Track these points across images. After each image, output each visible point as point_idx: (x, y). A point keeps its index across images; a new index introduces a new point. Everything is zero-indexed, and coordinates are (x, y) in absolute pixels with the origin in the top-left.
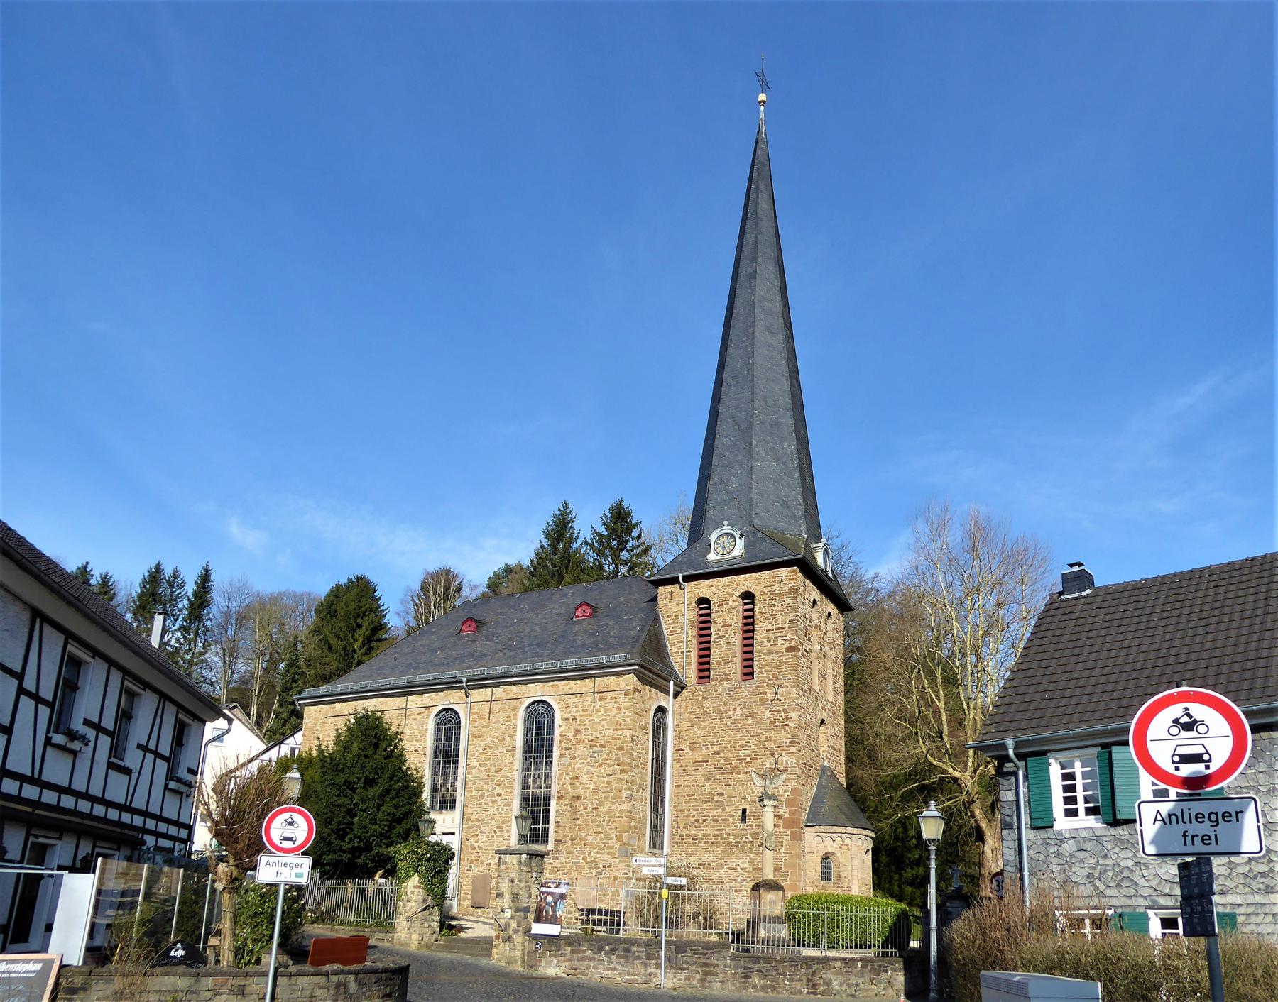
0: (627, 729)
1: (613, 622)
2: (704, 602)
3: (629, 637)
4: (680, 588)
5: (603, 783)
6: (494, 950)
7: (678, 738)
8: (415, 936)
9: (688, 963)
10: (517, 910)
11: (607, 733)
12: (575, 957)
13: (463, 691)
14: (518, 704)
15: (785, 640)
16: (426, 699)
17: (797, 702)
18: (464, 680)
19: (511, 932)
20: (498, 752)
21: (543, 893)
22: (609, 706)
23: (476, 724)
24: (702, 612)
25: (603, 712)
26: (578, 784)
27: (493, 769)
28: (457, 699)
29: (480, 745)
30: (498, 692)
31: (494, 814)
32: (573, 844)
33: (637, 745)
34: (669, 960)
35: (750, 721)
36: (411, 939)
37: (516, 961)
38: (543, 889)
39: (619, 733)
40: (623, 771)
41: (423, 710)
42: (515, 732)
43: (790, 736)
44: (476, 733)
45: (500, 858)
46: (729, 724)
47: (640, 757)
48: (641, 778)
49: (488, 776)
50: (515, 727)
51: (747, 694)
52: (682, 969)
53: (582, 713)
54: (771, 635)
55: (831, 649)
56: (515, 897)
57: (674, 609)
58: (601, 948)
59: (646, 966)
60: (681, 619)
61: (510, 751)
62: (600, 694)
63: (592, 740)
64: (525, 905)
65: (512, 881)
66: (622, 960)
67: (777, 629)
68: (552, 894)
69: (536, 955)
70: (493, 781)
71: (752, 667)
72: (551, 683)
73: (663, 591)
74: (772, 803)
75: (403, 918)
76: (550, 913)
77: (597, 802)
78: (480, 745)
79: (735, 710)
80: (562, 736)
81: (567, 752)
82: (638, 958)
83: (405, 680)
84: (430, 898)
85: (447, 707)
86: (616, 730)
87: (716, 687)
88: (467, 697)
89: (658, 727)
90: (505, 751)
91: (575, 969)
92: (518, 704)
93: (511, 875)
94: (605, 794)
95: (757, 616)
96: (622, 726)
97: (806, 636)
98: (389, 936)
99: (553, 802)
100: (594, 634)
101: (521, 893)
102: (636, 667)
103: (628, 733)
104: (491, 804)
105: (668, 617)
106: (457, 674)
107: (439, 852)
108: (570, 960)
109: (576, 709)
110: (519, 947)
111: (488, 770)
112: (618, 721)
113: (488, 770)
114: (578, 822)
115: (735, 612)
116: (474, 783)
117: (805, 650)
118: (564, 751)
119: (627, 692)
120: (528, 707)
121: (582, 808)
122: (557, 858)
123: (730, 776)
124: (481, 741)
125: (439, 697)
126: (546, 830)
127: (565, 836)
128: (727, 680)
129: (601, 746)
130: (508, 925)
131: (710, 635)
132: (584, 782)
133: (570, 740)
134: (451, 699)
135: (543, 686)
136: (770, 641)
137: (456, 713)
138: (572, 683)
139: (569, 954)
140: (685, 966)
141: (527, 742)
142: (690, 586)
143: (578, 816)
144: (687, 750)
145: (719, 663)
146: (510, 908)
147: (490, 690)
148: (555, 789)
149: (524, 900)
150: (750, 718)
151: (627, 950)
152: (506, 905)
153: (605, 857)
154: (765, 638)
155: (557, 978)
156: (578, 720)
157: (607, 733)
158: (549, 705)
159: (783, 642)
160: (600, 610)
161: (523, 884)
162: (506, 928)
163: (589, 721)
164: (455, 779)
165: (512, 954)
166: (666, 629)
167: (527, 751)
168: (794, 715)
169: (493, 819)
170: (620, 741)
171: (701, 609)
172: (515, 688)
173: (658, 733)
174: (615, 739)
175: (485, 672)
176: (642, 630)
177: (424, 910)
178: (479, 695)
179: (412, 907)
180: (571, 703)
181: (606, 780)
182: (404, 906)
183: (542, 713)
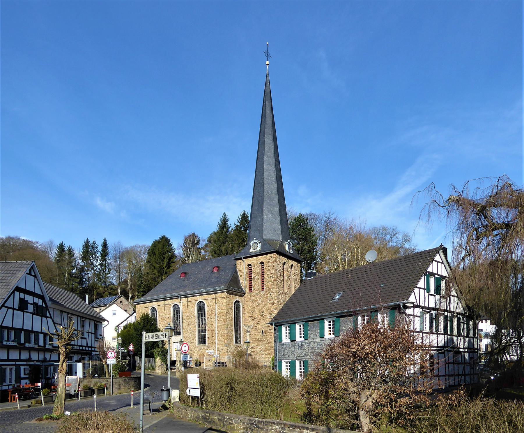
16: (170, 302)
18: (179, 296)
23: (184, 309)
27: (190, 322)
35: (264, 304)
39: (223, 310)
40: (224, 322)
48: (230, 323)
55: (294, 276)
57: (241, 268)
62: (217, 299)
74: (249, 333)
75: (157, 367)
81: (209, 317)
83: (163, 296)
86: (222, 310)
87: (254, 293)
95: (265, 270)
99: (207, 332)
106: (177, 294)
111: (188, 323)
113: (188, 323)
114: (214, 337)
115: (258, 269)
116: (185, 327)
119: (224, 298)
120: (198, 303)
126: (205, 340)
127: (210, 342)
128: (257, 291)
130: (179, 368)
131: (252, 276)
134: (176, 302)
141: (199, 314)
142: (245, 260)
144: (247, 313)
145: (254, 285)
147: (187, 298)
148: (207, 328)
152: (178, 363)
153: (221, 347)
160: (221, 269)
164: (180, 326)
168: (276, 301)
175: (185, 293)
176: (231, 276)
178: (185, 300)
180: (209, 302)
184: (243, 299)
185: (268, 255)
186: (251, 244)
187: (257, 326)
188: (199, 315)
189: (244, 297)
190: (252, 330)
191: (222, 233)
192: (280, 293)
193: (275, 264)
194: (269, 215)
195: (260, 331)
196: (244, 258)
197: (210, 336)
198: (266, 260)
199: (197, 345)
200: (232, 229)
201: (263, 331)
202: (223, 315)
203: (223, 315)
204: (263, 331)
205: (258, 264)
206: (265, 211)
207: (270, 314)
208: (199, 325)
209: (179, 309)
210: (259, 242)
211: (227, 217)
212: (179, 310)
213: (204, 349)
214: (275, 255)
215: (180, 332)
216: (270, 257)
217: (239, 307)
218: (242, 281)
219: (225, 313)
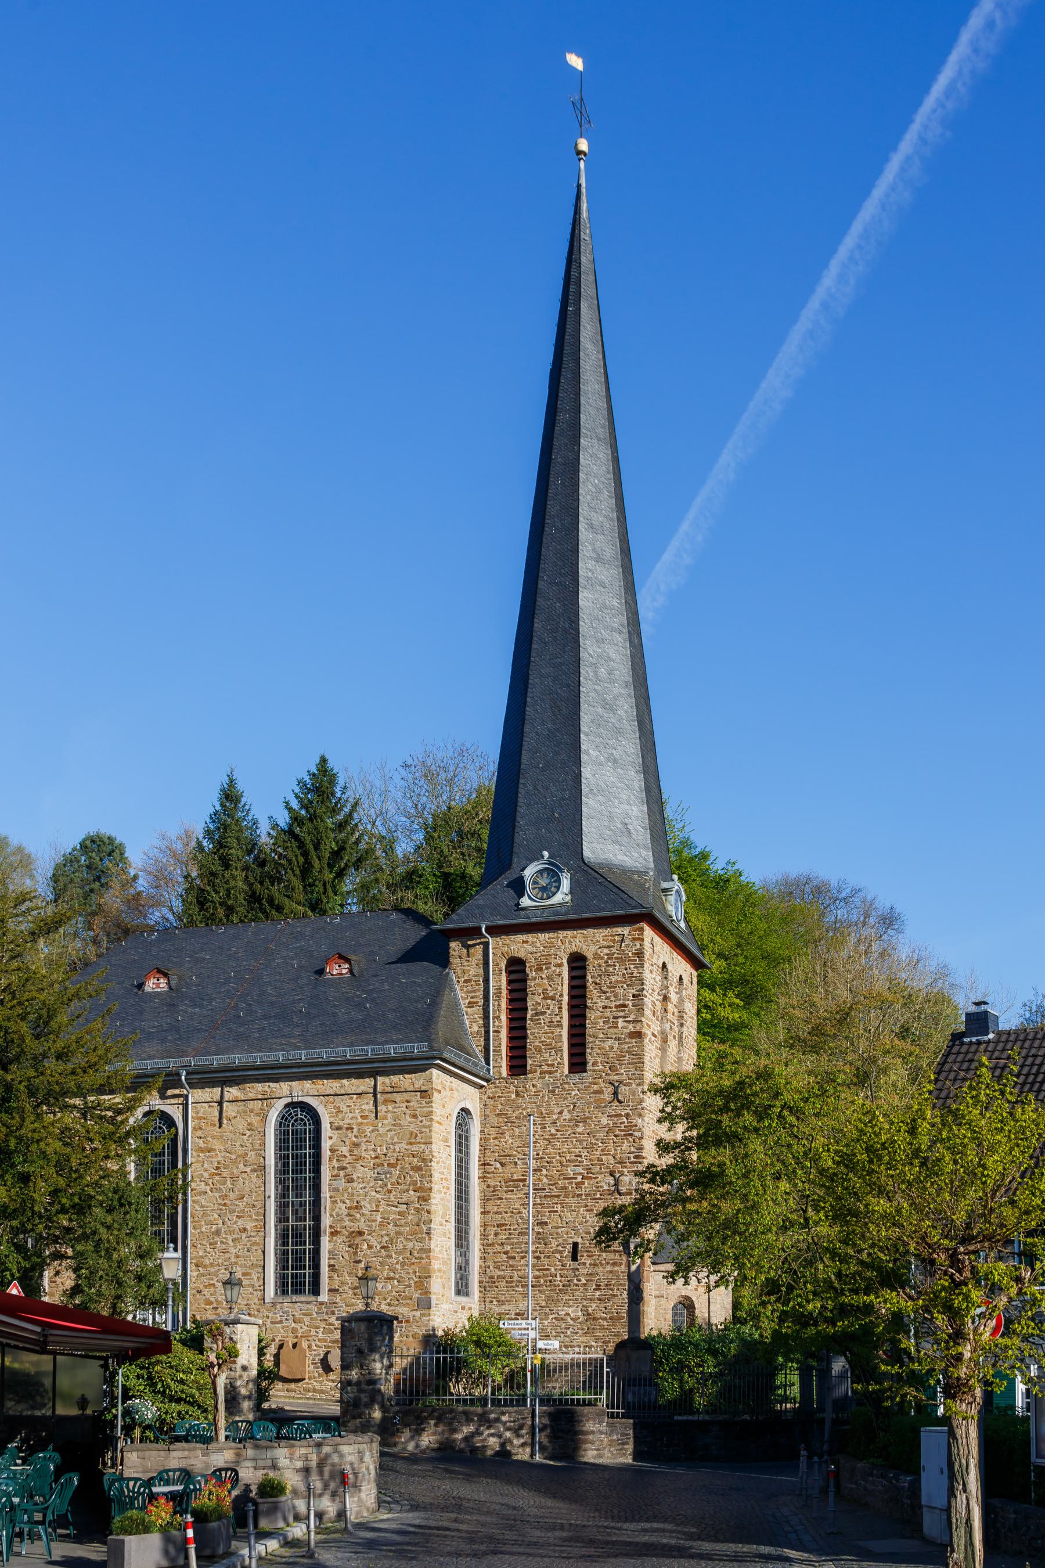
7: (484, 1148)
35: (580, 1129)
39: (415, 1148)
43: (633, 1149)
46: (553, 1131)
47: (442, 1179)
63: (376, 1157)
67: (616, 1007)
70: (232, 1211)
79: (561, 1113)
81: (342, 1173)
86: (411, 1144)
87: (534, 1081)
89: (460, 1136)
90: (248, 1169)
95: (590, 986)
96: (418, 1139)
100: (360, 1005)
104: (231, 1244)
109: (351, 1115)
112: (412, 1133)
117: (654, 1035)
118: (336, 1172)
122: (333, 1313)
123: (555, 1200)
128: (550, 1073)
133: (345, 1156)
141: (282, 1159)
145: (538, 1050)
150: (581, 1125)
156: (355, 1130)
159: (626, 1024)
167: (282, 1172)
172: (259, 1086)
183: (302, 1120)
201: (575, 1245)
204: (575, 1245)
207: (612, 1174)
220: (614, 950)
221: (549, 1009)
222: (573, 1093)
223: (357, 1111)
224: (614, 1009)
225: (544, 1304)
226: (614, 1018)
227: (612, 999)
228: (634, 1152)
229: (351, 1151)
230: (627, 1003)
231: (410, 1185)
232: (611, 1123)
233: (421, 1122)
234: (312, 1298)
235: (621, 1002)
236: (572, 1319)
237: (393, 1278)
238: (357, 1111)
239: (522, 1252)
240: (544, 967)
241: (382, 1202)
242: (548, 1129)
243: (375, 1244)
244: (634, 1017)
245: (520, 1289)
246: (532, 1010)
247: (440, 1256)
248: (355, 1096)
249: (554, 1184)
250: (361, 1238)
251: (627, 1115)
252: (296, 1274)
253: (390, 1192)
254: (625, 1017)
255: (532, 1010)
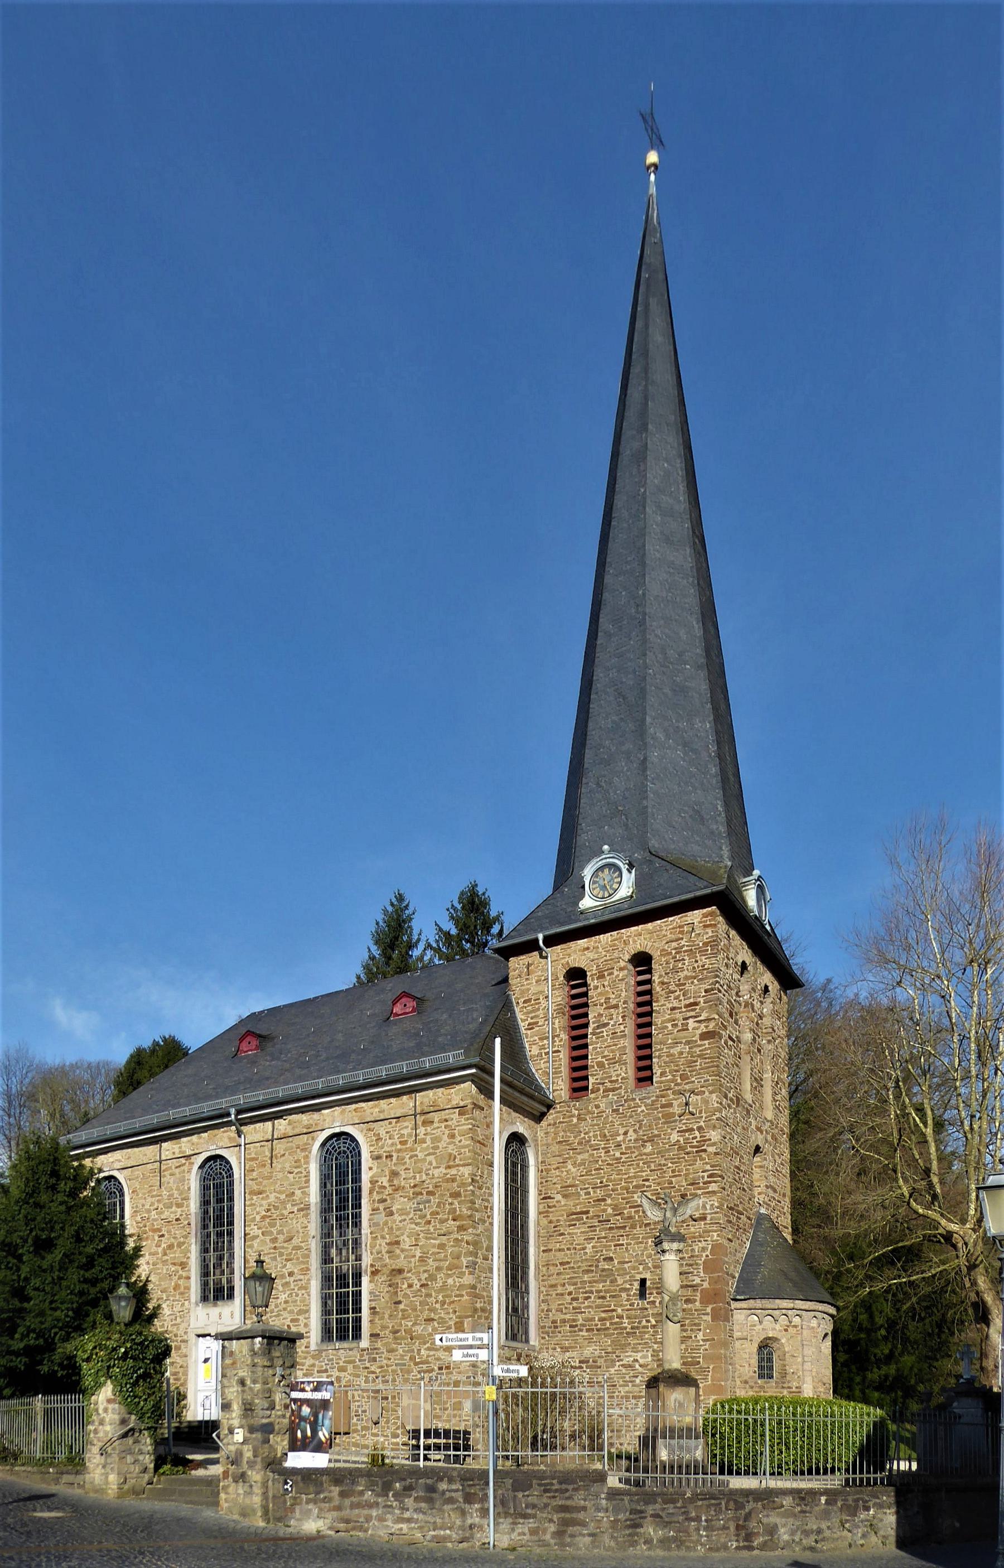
0: (464, 1165)
1: (445, 1016)
2: (576, 975)
3: (466, 1032)
4: (541, 957)
5: (434, 1246)
6: (223, 1496)
8: (112, 1478)
9: (534, 1506)
10: (252, 1430)
11: (436, 1173)
12: (347, 1502)
13: (233, 1128)
14: (310, 1141)
15: (699, 1022)
16: (185, 1144)
17: (718, 1115)
18: (233, 1111)
19: (245, 1466)
20: (286, 1213)
21: (295, 1401)
22: (438, 1132)
23: (255, 1174)
24: (574, 992)
25: (429, 1142)
26: (398, 1251)
27: (281, 1238)
28: (226, 1140)
29: (261, 1205)
30: (282, 1125)
31: (286, 1302)
32: (395, 1338)
33: (480, 1188)
34: (501, 1502)
35: (649, 1148)
36: (107, 1483)
37: (254, 1511)
38: (295, 1395)
39: (454, 1171)
40: (461, 1228)
41: (183, 1160)
42: (308, 1181)
43: (708, 1167)
44: (255, 1187)
45: (223, 1347)
46: (618, 1155)
49: (275, 1248)
50: (307, 1176)
51: (643, 1108)
52: (525, 1516)
53: (399, 1147)
54: (678, 1016)
55: (769, 1042)
56: (248, 1409)
57: (534, 989)
58: (387, 1487)
59: (463, 1513)
60: (543, 1003)
61: (302, 1210)
62: (424, 1116)
63: (415, 1186)
64: (265, 1421)
65: (242, 1382)
66: (423, 1505)
67: (686, 1006)
68: (308, 1402)
69: (285, 1502)
70: (281, 1254)
71: (650, 1068)
72: (354, 1106)
73: (517, 964)
74: (675, 1246)
75: (95, 1450)
76: (309, 1433)
77: (426, 1275)
78: (261, 1205)
79: (626, 1133)
80: (373, 1182)
81: (381, 1206)
82: (451, 1501)
83: (154, 1119)
84: (133, 1417)
85: (213, 1153)
86: (449, 1167)
87: (598, 1101)
88: (240, 1136)
89: (514, 1165)
90: (295, 1209)
91: (347, 1521)
92: (310, 1141)
93: (242, 1373)
94: (437, 1264)
95: (657, 988)
97: (731, 1015)
98: (79, 1479)
99: (365, 1280)
101: (257, 1401)
102: (474, 1071)
103: (466, 1171)
105: (524, 1002)
106: (222, 1103)
107: (141, 1343)
108: (339, 1508)
109: (390, 1142)
110: (257, 1490)
111: (274, 1240)
112: (450, 1155)
113: (274, 1240)
114: (402, 1306)
117: (730, 1038)
118: (376, 1205)
119: (462, 1110)
120: (323, 1144)
121: (405, 1286)
122: (374, 1360)
124: (263, 1199)
125: (202, 1141)
126: (358, 1321)
127: (384, 1327)
128: (613, 1090)
129: (429, 1193)
130: (239, 1454)
131: (586, 1026)
132: (407, 1247)
133: (385, 1187)
135: (343, 1112)
136: (676, 1025)
137: (228, 1162)
138: (383, 1103)
139: (337, 1497)
140: (529, 1511)
141: (325, 1195)
142: (555, 952)
143: (400, 1298)
144: (559, 1197)
145: (601, 1065)
146: (241, 1427)
147: (269, 1124)
148: (367, 1260)
149: (261, 1413)
150: (648, 1144)
151: (432, 1489)
152: (236, 1422)
154: (669, 1020)
155: (319, 1535)
156: (394, 1158)
157: (436, 1173)
158: (353, 1139)
159: (697, 1025)
161: (258, 1386)
162: (237, 1459)
163: (411, 1157)
165: (248, 1501)
166: (523, 1021)
167: (325, 1210)
169: (285, 1309)
170: (455, 1185)
171: (573, 987)
172: (304, 1118)
173: (514, 1173)
174: (447, 1181)
175: (260, 1096)
176: (485, 1021)
177: (125, 1435)
179: (106, 1433)
180: (382, 1133)
181: (437, 1242)
182: (96, 1431)
183: (345, 1152)
184: (540, 1134)
185: (675, 920)
186: (588, 873)
187: (611, 1259)
188: (330, 1202)
189: (544, 1123)
190: (586, 1278)
191: (390, 958)
192: (731, 1100)
193: (715, 955)
194: (669, 748)
195: (631, 1282)
196: (552, 941)
197: (385, 1299)
198: (661, 944)
199: (313, 1347)
200: (429, 946)
201: (643, 1282)
202: (456, 1195)
203: (456, 1195)
204: (643, 1282)
205: (622, 964)
206: (655, 731)
208: (326, 1249)
209: (231, 1176)
210: (631, 866)
211: (408, 905)
212: (231, 1184)
213: (350, 1367)
214: (711, 914)
215: (231, 1289)
216: (686, 929)
217: (525, 1167)
218: (535, 1050)
219: (463, 1185)
220: (683, 943)
221: (611, 1019)
222: (640, 1110)
223: (396, 1137)
224: (684, 1010)
225: (610, 1350)
226: (685, 1019)
227: (682, 998)
228: (708, 1171)
229: (390, 1181)
230: (699, 999)
231: (449, 1213)
232: (681, 1139)
233: (460, 1141)
234: (354, 1345)
235: (692, 1000)
236: (641, 1366)
237: (433, 1320)
238: (396, 1137)
239: (586, 1293)
240: (606, 973)
241: (422, 1235)
242: (612, 1153)
243: (416, 1282)
244: (706, 1015)
245: (584, 1333)
246: (594, 1023)
247: (485, 1294)
248: (395, 1120)
249: (619, 1214)
250: (401, 1276)
251: (700, 1129)
252: (341, 1318)
253: (429, 1222)
254: (696, 1017)
255: (594, 1023)
